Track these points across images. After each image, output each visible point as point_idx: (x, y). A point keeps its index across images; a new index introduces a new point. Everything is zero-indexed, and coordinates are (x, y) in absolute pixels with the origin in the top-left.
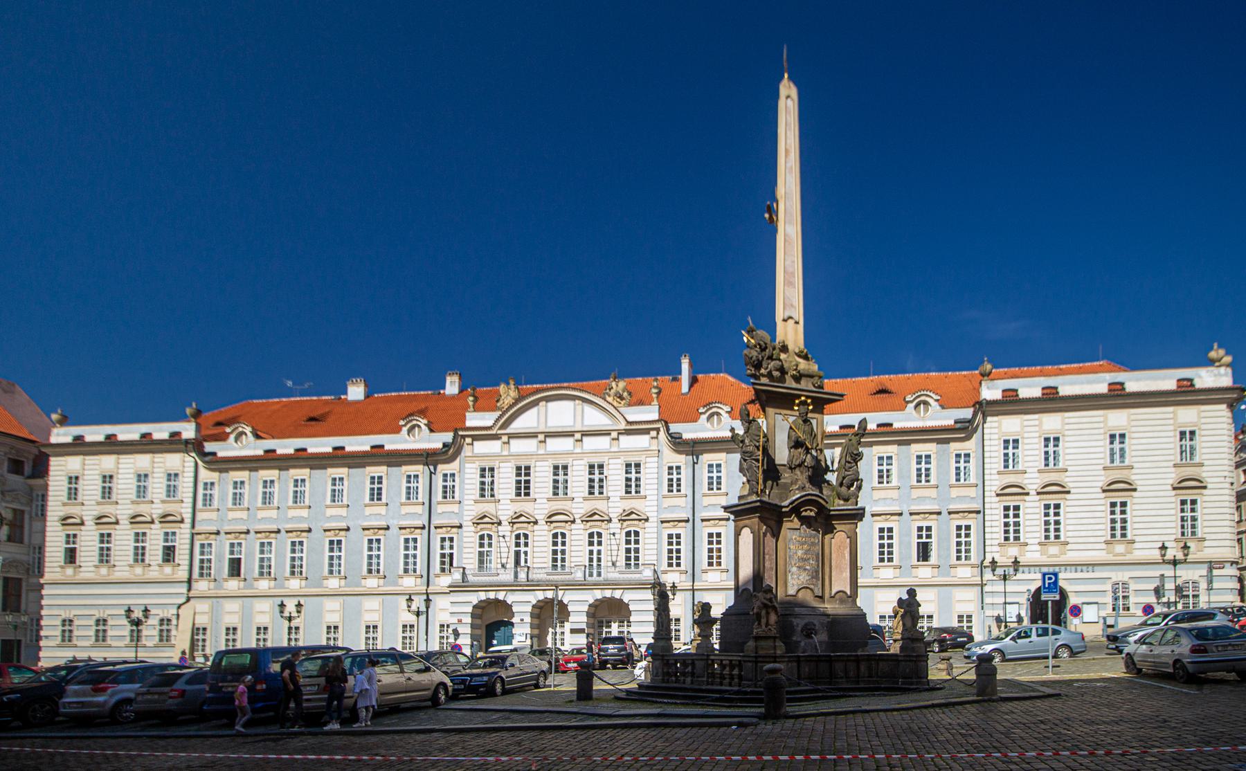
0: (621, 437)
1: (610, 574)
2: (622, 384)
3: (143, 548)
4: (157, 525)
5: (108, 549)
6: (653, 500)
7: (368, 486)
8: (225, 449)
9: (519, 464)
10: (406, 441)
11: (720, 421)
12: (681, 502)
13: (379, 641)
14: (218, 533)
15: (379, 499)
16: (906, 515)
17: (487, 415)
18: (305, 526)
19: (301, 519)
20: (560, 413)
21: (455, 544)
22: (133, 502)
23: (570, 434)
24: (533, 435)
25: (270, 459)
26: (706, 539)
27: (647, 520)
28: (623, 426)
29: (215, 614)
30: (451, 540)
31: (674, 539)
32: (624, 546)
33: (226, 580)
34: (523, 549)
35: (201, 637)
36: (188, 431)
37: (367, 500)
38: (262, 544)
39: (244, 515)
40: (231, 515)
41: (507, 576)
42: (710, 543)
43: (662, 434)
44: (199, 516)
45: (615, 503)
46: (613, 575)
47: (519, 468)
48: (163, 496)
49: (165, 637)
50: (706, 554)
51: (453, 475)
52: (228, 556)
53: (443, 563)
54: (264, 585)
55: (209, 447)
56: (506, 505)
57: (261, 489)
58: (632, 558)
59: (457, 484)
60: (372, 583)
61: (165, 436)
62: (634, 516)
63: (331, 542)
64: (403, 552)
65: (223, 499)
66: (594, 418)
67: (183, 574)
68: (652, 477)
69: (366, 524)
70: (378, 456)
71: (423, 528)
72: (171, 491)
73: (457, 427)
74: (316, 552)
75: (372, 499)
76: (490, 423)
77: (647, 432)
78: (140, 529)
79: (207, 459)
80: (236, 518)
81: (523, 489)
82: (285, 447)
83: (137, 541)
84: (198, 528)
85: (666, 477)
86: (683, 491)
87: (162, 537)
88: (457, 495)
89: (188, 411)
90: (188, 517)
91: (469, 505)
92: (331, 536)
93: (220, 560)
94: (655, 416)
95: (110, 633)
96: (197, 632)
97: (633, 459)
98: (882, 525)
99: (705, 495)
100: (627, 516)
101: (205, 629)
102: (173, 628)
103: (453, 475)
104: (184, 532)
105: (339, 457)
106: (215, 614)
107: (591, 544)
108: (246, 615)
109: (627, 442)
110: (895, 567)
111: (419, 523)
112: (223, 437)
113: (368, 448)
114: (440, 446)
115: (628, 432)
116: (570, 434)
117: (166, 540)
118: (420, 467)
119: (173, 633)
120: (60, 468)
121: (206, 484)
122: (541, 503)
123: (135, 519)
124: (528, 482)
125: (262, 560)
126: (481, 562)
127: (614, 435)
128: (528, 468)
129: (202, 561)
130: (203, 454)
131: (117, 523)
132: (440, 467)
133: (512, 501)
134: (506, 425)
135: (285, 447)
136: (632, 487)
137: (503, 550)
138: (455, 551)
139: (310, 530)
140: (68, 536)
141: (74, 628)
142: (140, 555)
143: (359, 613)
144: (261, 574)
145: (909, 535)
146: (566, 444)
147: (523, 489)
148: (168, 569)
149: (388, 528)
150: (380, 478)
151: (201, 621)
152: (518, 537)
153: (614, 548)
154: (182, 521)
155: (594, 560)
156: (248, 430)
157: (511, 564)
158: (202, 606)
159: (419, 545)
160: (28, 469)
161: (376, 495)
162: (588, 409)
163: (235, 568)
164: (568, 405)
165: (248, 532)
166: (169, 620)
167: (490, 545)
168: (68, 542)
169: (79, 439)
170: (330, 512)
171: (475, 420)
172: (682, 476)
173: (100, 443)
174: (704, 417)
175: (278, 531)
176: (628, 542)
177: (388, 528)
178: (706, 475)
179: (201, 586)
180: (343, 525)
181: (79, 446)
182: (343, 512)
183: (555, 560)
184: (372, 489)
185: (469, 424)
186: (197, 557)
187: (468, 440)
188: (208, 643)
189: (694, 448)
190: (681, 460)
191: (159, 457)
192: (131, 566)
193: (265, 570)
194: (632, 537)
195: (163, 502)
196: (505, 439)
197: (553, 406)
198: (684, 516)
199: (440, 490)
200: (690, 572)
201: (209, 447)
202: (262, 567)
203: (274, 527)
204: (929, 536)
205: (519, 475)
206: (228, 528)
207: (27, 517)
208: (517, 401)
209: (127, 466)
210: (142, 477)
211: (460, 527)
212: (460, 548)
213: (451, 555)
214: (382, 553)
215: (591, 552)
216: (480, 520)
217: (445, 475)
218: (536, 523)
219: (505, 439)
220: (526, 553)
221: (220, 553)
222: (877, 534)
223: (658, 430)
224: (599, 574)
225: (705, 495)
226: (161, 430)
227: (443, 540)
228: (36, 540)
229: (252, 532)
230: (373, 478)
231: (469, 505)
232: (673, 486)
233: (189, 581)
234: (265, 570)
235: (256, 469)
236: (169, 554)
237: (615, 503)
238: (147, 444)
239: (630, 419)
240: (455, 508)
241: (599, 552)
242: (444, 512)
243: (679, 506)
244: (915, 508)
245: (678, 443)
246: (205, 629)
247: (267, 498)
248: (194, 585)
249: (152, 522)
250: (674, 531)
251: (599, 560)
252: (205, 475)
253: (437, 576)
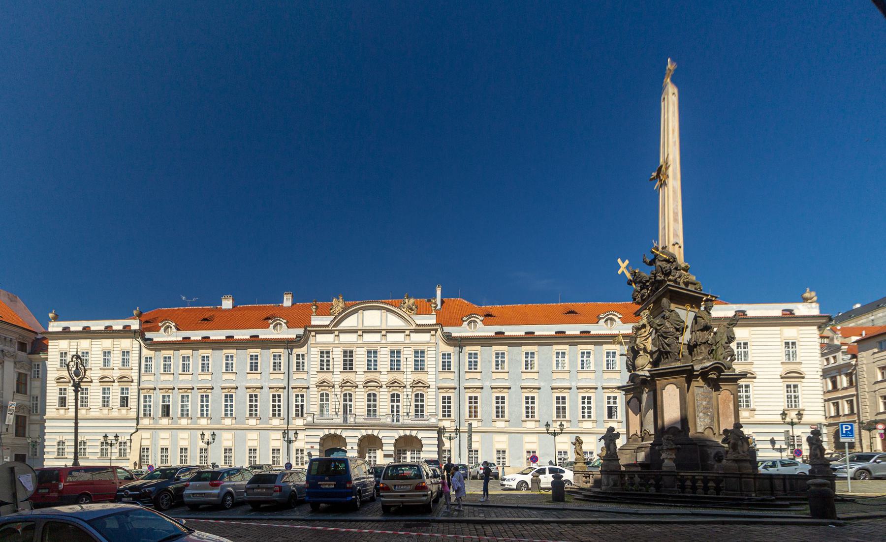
0: (412, 334)
1: (404, 420)
2: (412, 301)
3: (108, 398)
4: (116, 384)
5: (86, 398)
6: (432, 375)
7: (249, 361)
8: (159, 337)
9: (345, 349)
10: (273, 334)
11: (475, 326)
12: (451, 376)
13: (257, 459)
14: (155, 389)
15: (256, 370)
16: (600, 389)
17: (324, 318)
18: (209, 385)
19: (206, 381)
20: (372, 318)
21: (305, 399)
22: (101, 369)
23: (378, 331)
24: (354, 331)
25: (186, 343)
26: (467, 400)
27: (429, 387)
28: (414, 327)
29: (154, 439)
30: (302, 396)
31: (446, 400)
32: (413, 403)
34: (348, 403)
35: (145, 454)
36: (135, 325)
37: (248, 370)
38: (183, 397)
39: (171, 378)
40: (163, 378)
41: (339, 420)
42: (470, 403)
43: (439, 332)
44: (143, 378)
45: (408, 376)
46: (407, 421)
47: (345, 352)
48: (120, 365)
49: (122, 454)
50: (467, 410)
51: (303, 355)
52: (161, 404)
53: (297, 411)
54: (184, 422)
55: (148, 335)
56: (337, 376)
57: (181, 362)
58: (419, 411)
59: (305, 361)
60: (252, 422)
62: (420, 384)
63: (226, 396)
64: (271, 403)
65: (158, 368)
66: (394, 321)
67: (133, 414)
68: (432, 360)
69: (248, 385)
70: (254, 342)
71: (284, 388)
72: (125, 362)
73: (307, 325)
74: (217, 401)
75: (251, 370)
76: (327, 323)
77: (428, 331)
78: (106, 385)
79: (148, 342)
80: (166, 380)
81: (348, 365)
82: (196, 335)
83: (104, 393)
84: (142, 386)
85: (441, 360)
86: (452, 370)
87: (120, 391)
88: (305, 368)
89: (135, 312)
90: (136, 379)
91: (313, 375)
92: (226, 392)
94: (434, 322)
95: (88, 450)
96: (143, 450)
97: (419, 348)
98: (584, 395)
99: (466, 372)
100: (416, 384)
101: (148, 449)
102: (128, 448)
103: (303, 355)
104: (133, 389)
105: (230, 342)
106: (154, 439)
107: (392, 401)
108: (174, 440)
109: (415, 337)
110: (593, 422)
111: (281, 385)
112: (157, 329)
113: (248, 337)
114: (295, 337)
115: (416, 331)
116: (378, 331)
117: (122, 393)
118: (282, 350)
119: (128, 451)
120: (56, 347)
121: (146, 358)
122: (360, 375)
123: (102, 380)
124: (351, 361)
125: (182, 406)
126: (322, 411)
127: (407, 332)
128: (351, 352)
129: (145, 406)
130: (145, 340)
131: (91, 382)
132: (295, 350)
133: (341, 372)
134: (336, 325)
135: (196, 336)
136: (419, 366)
137: (335, 404)
138: (305, 403)
139: (212, 389)
140: (61, 389)
141: (65, 447)
142: (105, 402)
143: (244, 441)
144: (182, 415)
145: (602, 401)
146: (376, 337)
147: (348, 365)
148: (124, 411)
149: (262, 388)
150: (257, 356)
151: (145, 443)
152: (345, 395)
153: (407, 403)
154: (132, 381)
155: (395, 412)
156: (173, 325)
157: (341, 412)
158: (146, 435)
159: (282, 399)
160: (29, 348)
161: (254, 367)
162: (390, 316)
163: (166, 411)
164: (376, 313)
165: (174, 389)
166: (125, 443)
167: (327, 400)
168: (61, 394)
169: (66, 330)
170: (225, 377)
171: (316, 321)
172: (452, 360)
173: (80, 332)
174: (466, 323)
175: (193, 389)
176: (416, 401)
177: (262, 388)
178: (467, 360)
179: (145, 422)
180: (234, 385)
181: (66, 333)
182: (233, 377)
183: (369, 411)
184: (251, 363)
185: (313, 323)
186: (142, 404)
187: (313, 333)
188: (150, 458)
189: (460, 343)
190: (451, 349)
192: (100, 409)
193: (184, 414)
194: (419, 398)
195: (120, 369)
196: (336, 333)
197: (367, 313)
198: (453, 385)
199: (295, 365)
200: (457, 420)
201: (148, 335)
202: (182, 411)
203: (190, 386)
204: (615, 403)
205: (345, 356)
206: (161, 386)
207: (28, 378)
208: (344, 310)
210: (106, 353)
211: (308, 388)
212: (309, 402)
213: (302, 406)
214: (258, 403)
215: (393, 407)
216: (321, 384)
217: (298, 355)
218: (357, 387)
219: (336, 333)
220: (350, 406)
221: (157, 401)
222: (580, 401)
223: (436, 330)
224: (398, 421)
225: (466, 372)
226: (118, 325)
227: (297, 396)
228: (36, 392)
230: (252, 356)
231: (313, 375)
232: (446, 366)
233: (138, 419)
234: (184, 414)
235: (178, 350)
236: (124, 402)
237: (408, 376)
238: (109, 333)
239: (418, 322)
240: (304, 376)
241: (398, 407)
242: (298, 379)
243: (450, 379)
244: (605, 385)
245: (449, 339)
246: (148, 449)
247: (185, 368)
248: (141, 421)
249: (114, 382)
250: (447, 395)
251: (398, 411)
252: (146, 352)
253: (294, 419)
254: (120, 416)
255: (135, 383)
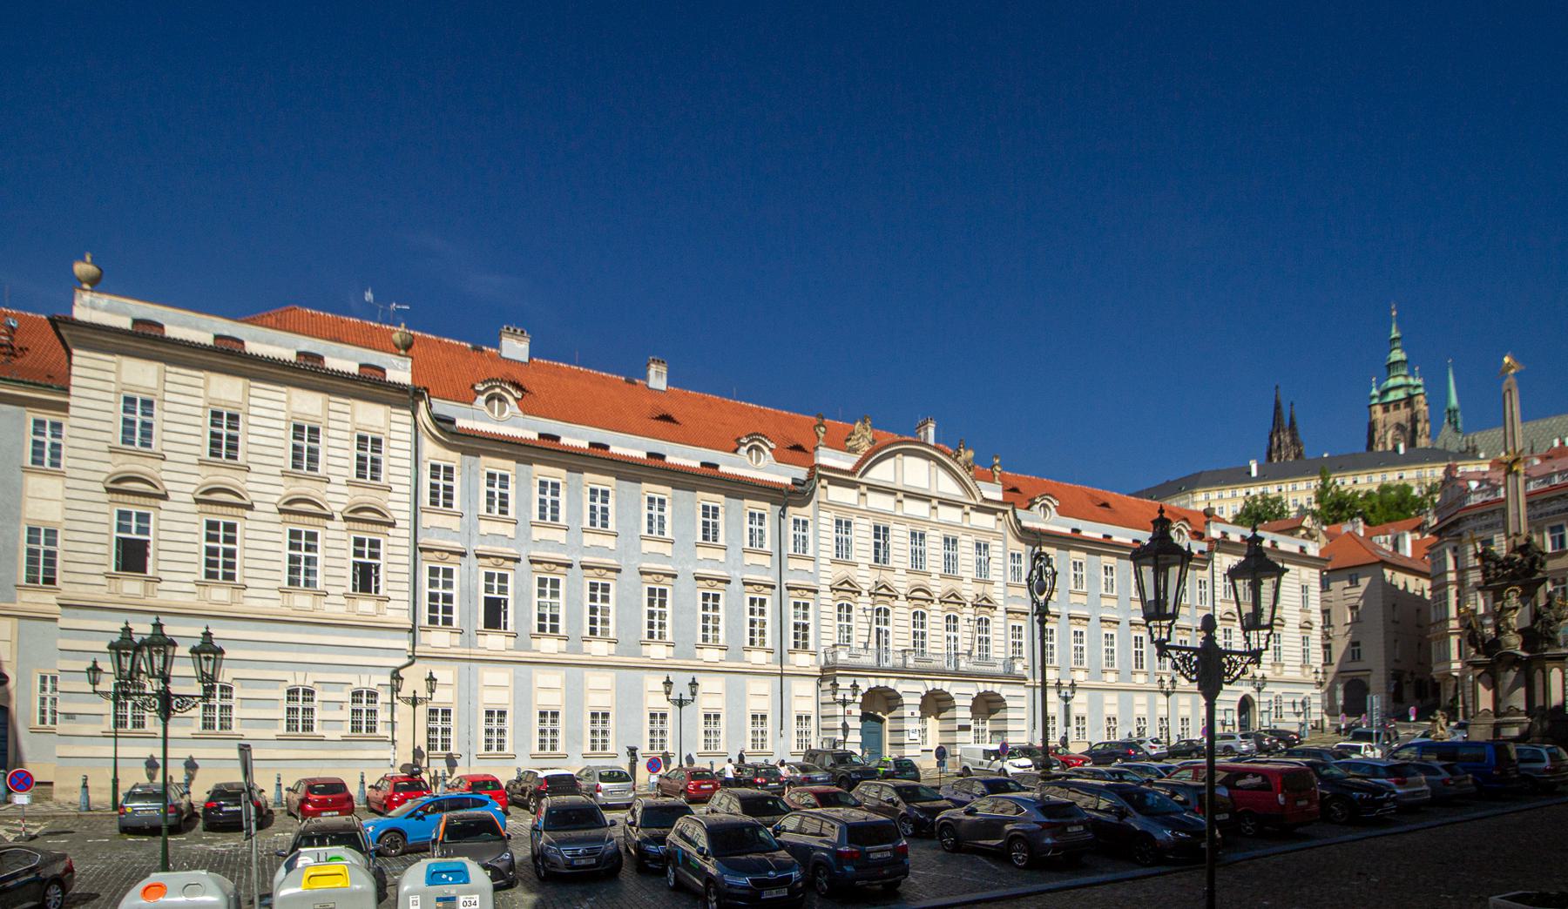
33: (478, 633)
36: (400, 372)
39: (509, 530)
44: (426, 520)
52: (483, 594)
61: (352, 368)
65: (470, 494)
80: (495, 533)
93: (468, 594)
117: (358, 554)
121: (435, 468)
129: (433, 597)
142: (300, 572)
148: (366, 605)
154: (392, 525)
163: (494, 614)
166: (373, 695)
179: (438, 639)
186: (425, 591)
191: (338, 403)
192: (281, 590)
193: (548, 624)
195: (349, 483)
209: (269, 412)
221: (469, 589)
229: (525, 561)
236: (366, 578)
248: (423, 637)
249: (331, 517)
252: (433, 452)
254: (353, 618)
255: (403, 532)
